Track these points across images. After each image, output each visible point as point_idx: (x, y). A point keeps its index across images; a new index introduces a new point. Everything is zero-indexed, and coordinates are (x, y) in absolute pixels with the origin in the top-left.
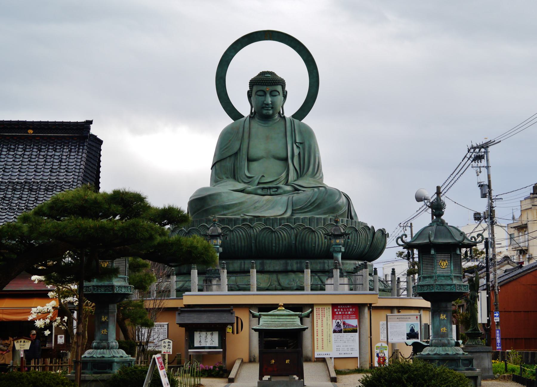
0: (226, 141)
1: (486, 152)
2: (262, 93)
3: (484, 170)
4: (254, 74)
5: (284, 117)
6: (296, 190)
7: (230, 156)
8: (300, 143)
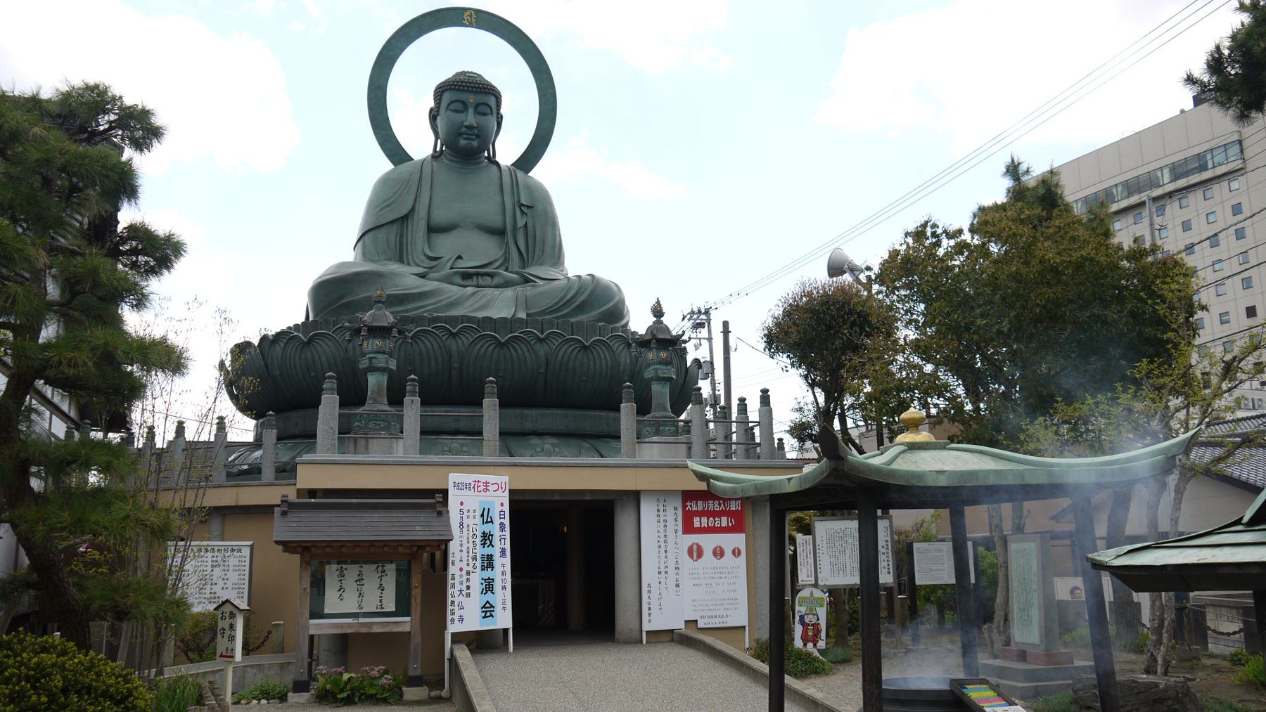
0: (385, 193)
1: (709, 320)
2: (458, 106)
3: (705, 343)
4: (447, 74)
5: (497, 164)
6: (527, 281)
7: (393, 222)
8: (528, 207)
